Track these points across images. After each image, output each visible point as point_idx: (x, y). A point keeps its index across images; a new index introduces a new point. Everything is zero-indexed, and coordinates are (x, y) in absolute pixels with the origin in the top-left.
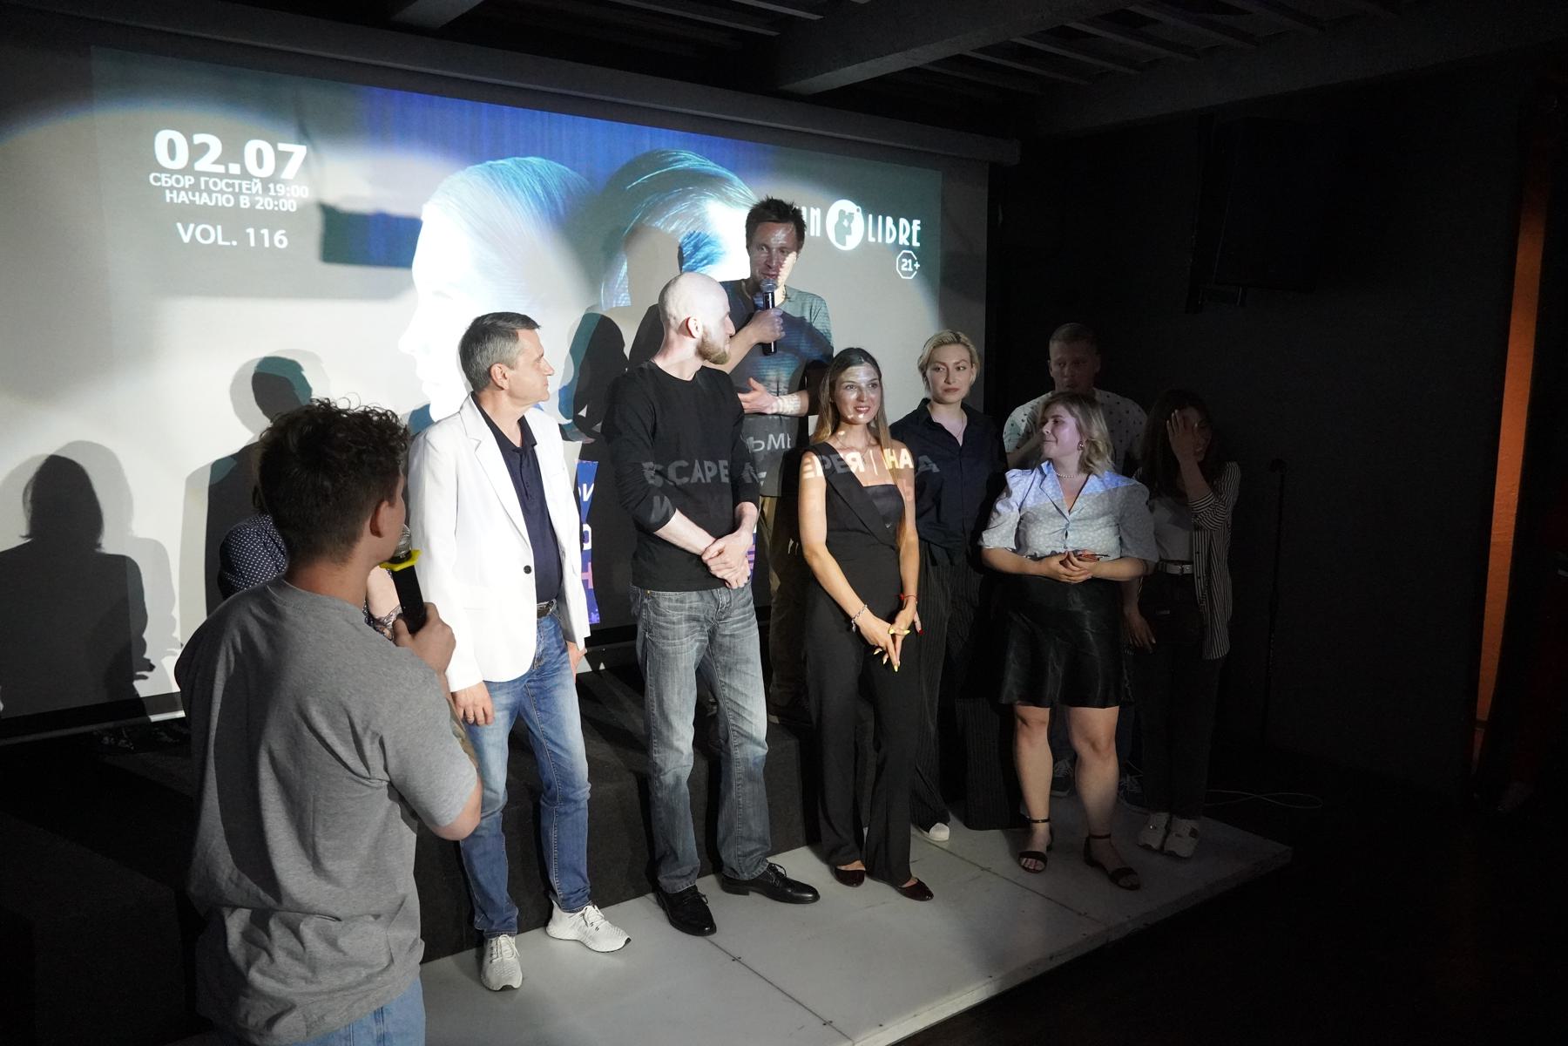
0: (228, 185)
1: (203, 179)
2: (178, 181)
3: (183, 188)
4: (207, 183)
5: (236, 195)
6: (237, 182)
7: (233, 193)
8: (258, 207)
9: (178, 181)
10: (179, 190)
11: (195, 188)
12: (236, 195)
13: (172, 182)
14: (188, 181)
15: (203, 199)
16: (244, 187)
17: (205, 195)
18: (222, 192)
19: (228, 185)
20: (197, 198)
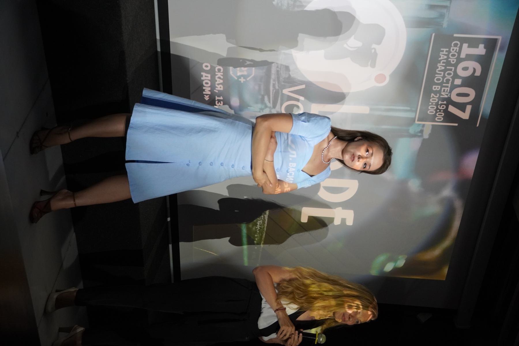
0: (448, 81)
1: (453, 68)
2: (453, 55)
3: (448, 58)
4: (451, 70)
5: (441, 84)
6: (449, 85)
7: (443, 82)
8: (432, 94)
9: (453, 55)
10: (448, 55)
11: (448, 63)
12: (441, 84)
13: (453, 52)
14: (453, 60)
15: (440, 67)
16: (446, 89)
17: (443, 68)
18: (444, 77)
19: (448, 81)
20: (441, 64)
